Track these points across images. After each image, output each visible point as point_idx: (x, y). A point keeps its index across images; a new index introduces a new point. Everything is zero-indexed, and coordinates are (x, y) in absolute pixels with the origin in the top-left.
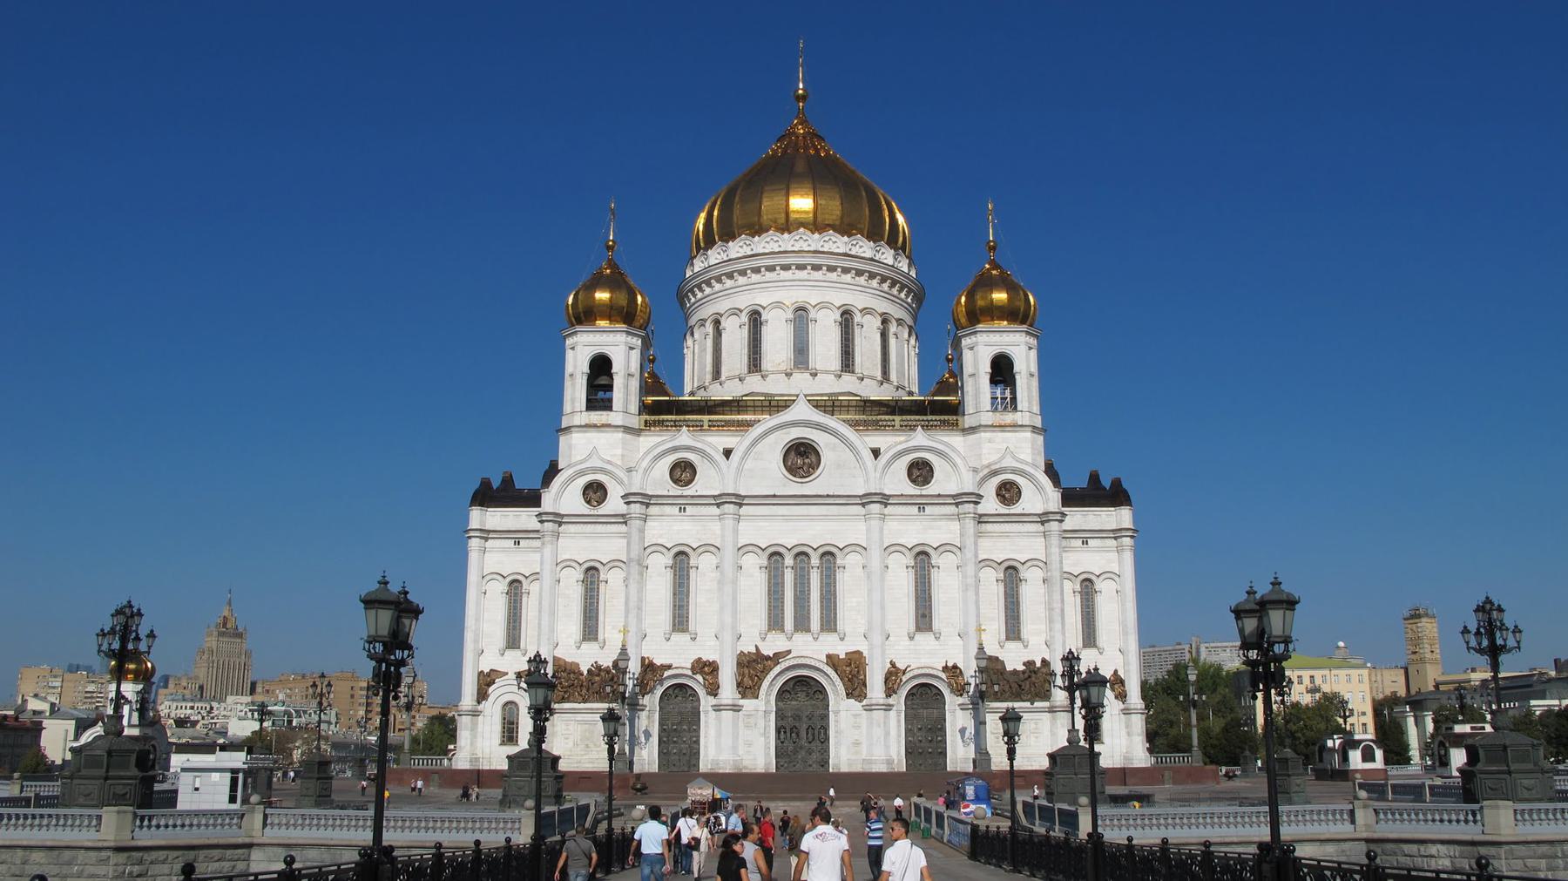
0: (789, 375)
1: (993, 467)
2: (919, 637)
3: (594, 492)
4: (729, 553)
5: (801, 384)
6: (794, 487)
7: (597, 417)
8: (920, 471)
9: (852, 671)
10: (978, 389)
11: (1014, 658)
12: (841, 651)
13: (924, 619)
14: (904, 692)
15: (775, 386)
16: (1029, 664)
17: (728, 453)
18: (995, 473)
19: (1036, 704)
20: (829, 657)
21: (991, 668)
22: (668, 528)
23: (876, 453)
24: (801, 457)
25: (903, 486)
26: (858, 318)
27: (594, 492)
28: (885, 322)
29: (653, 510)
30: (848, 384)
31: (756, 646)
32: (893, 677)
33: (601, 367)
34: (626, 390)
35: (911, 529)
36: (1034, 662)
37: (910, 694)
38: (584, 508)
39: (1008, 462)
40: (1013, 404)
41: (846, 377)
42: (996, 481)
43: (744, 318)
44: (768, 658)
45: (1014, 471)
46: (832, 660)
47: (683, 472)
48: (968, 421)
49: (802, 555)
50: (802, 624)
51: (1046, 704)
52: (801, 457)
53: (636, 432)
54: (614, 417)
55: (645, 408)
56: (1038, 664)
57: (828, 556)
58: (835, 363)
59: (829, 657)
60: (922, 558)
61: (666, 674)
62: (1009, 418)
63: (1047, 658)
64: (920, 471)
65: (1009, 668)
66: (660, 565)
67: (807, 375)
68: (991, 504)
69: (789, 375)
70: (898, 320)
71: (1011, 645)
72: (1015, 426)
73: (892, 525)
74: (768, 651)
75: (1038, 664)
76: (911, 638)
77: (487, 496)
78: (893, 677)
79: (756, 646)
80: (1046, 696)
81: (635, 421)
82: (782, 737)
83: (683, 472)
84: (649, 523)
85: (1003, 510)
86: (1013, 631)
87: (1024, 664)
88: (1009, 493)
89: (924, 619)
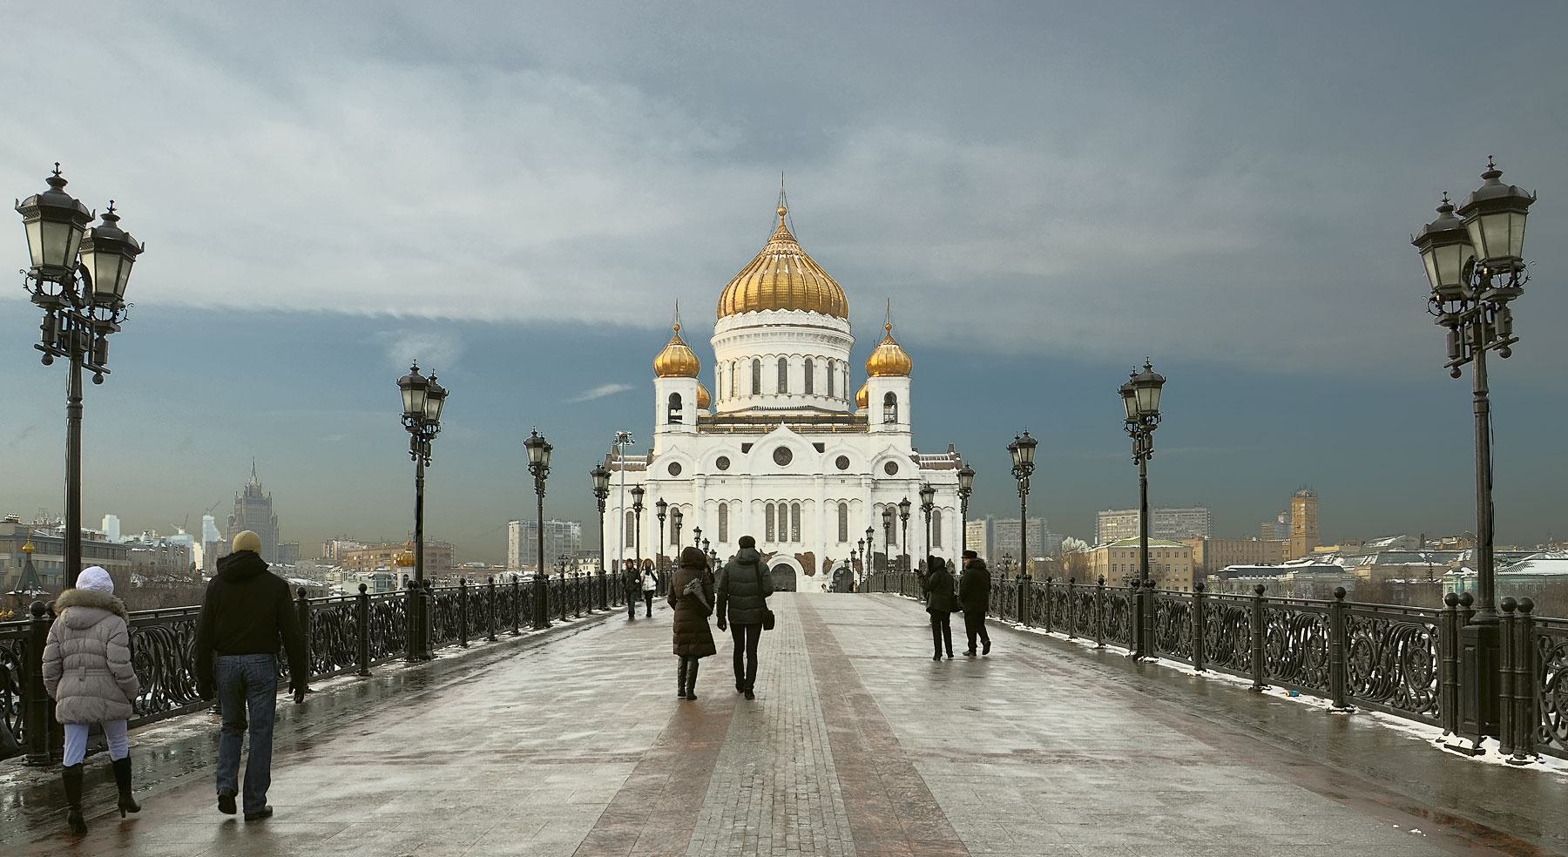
0: (776, 397)
1: (884, 455)
3: (675, 469)
4: (746, 502)
5: (783, 401)
6: (779, 469)
7: (672, 427)
8: (843, 462)
9: (807, 561)
10: (876, 412)
13: (843, 537)
14: (832, 572)
15: (769, 400)
17: (746, 448)
18: (884, 458)
20: (796, 554)
21: (880, 559)
22: (718, 492)
23: (820, 448)
24: (783, 456)
26: (815, 362)
27: (675, 469)
28: (831, 364)
29: (709, 482)
30: (809, 400)
32: (828, 564)
34: (689, 412)
35: (839, 491)
38: (670, 477)
39: (891, 452)
40: (895, 421)
41: (809, 397)
42: (885, 462)
43: (750, 363)
45: (894, 457)
46: (798, 556)
47: (723, 463)
48: (872, 429)
49: (783, 506)
50: (783, 539)
52: (783, 456)
53: (695, 436)
55: (700, 421)
58: (803, 391)
59: (796, 554)
60: (843, 509)
62: (893, 427)
64: (843, 462)
66: (713, 509)
67: (785, 397)
68: (883, 475)
69: (776, 397)
72: (895, 433)
73: (828, 488)
74: (766, 552)
78: (828, 564)
81: (694, 430)
83: (723, 463)
84: (707, 488)
85: (889, 477)
88: (891, 468)
89: (843, 537)
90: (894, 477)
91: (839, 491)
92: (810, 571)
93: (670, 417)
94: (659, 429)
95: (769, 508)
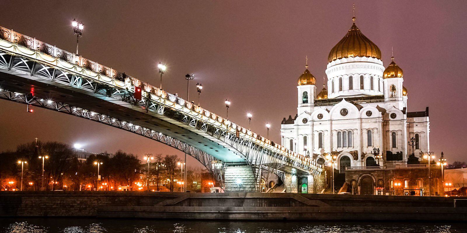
2: (369, 147)
3: (305, 121)
9: (355, 155)
11: (394, 151)
12: (353, 150)
14: (366, 158)
16: (398, 153)
19: (399, 161)
24: (344, 112)
25: (364, 116)
30: (362, 92)
31: (336, 150)
32: (363, 155)
33: (305, 95)
34: (311, 99)
36: (399, 152)
37: (367, 159)
44: (338, 152)
46: (351, 153)
47: (320, 116)
49: (344, 132)
51: (401, 161)
54: (309, 104)
55: (316, 102)
56: (400, 153)
57: (349, 132)
61: (318, 156)
63: (402, 151)
65: (393, 154)
67: (352, 90)
70: (375, 75)
71: (394, 149)
75: (400, 153)
76: (367, 148)
77: (285, 122)
78: (363, 155)
79: (336, 150)
80: (402, 159)
82: (341, 168)
86: (394, 146)
87: (397, 152)
90: (394, 119)
91: (367, 126)
92: (356, 158)
93: (303, 101)
94: (299, 106)
95: (339, 133)
